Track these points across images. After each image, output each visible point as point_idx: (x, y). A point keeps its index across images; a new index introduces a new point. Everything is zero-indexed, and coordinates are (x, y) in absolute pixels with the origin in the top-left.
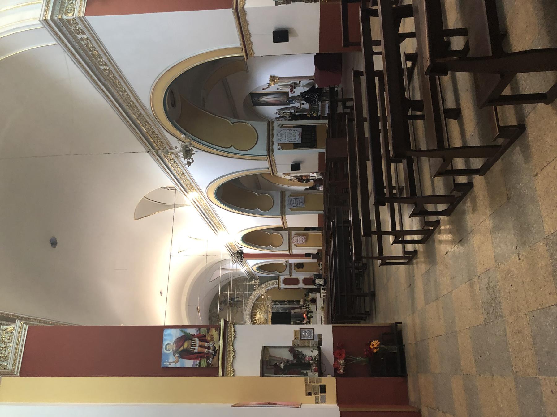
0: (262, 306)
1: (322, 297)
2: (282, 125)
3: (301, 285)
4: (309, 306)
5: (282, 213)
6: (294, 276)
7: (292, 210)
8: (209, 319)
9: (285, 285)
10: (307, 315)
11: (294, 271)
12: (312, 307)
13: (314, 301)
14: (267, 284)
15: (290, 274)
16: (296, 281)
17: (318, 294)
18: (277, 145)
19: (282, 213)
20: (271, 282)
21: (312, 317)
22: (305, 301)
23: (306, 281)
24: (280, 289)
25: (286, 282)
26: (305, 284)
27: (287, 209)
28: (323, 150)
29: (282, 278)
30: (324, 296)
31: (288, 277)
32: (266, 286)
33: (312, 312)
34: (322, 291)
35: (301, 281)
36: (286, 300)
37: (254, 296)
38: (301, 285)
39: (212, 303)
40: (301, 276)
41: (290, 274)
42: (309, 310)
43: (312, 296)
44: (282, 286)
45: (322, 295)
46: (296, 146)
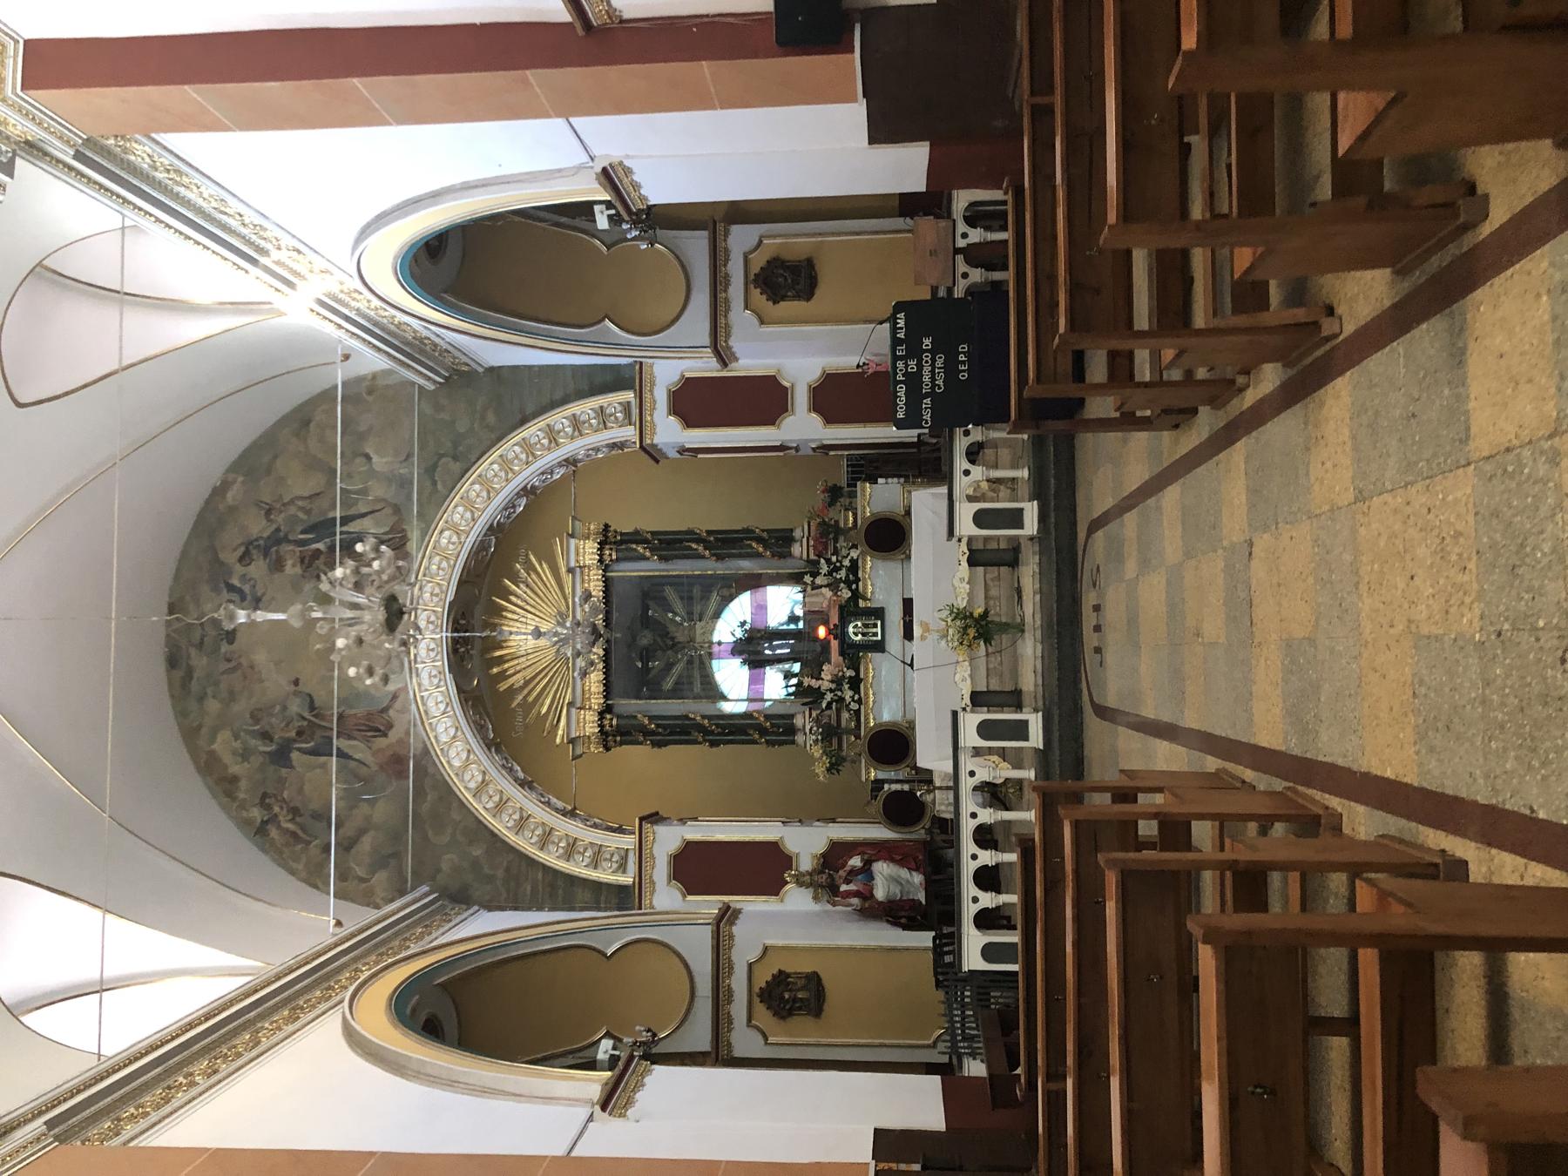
0: (544, 570)
1: (966, 526)
3: (802, 426)
4: (854, 567)
6: (750, 361)
8: (173, 662)
9: (689, 423)
10: (839, 632)
11: (740, 318)
12: (880, 581)
13: (890, 536)
14: (559, 418)
15: (723, 356)
17: (926, 504)
20: (585, 408)
21: (879, 647)
22: (828, 534)
23: (834, 396)
24: (652, 453)
25: (694, 402)
26: (830, 419)
29: (666, 373)
30: (981, 519)
31: (704, 366)
32: (552, 435)
33: (879, 613)
34: (968, 477)
35: (801, 399)
36: (702, 525)
37: (469, 504)
38: (802, 426)
39: (184, 554)
40: (795, 352)
41: (723, 356)
42: (856, 595)
43: (879, 496)
44: (669, 432)
45: (965, 513)
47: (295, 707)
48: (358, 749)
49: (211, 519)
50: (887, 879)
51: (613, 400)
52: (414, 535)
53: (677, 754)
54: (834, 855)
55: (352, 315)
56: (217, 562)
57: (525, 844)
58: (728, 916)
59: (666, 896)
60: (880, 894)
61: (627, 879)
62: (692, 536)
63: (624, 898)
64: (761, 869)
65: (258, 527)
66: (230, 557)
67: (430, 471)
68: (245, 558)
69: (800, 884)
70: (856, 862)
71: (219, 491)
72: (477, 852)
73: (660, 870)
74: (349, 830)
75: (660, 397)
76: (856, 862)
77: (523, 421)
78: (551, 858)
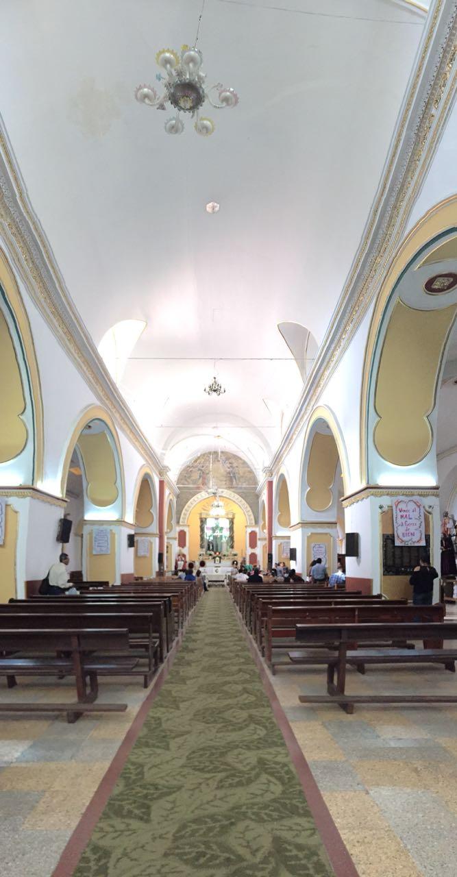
2: (430, 513)
5: (304, 524)
6: (259, 543)
7: (308, 538)
15: (259, 539)
16: (253, 544)
18: (389, 504)
19: (304, 524)
20: (252, 517)
23: (253, 556)
27: (310, 531)
28: (376, 591)
29: (257, 530)
31: (258, 537)
33: (220, 562)
35: (253, 551)
36: (235, 534)
38: (250, 551)
46: (388, 540)
47: (207, 471)
48: (201, 481)
49: (236, 458)
50: (181, 564)
51: (253, 522)
52: (233, 490)
53: (199, 529)
54: (184, 556)
55: (282, 453)
56: (230, 458)
57: (186, 507)
58: (175, 539)
59: (178, 529)
60: (179, 563)
61: (181, 523)
62: (233, 533)
63: (178, 522)
64: (182, 543)
65: (235, 465)
66: (230, 461)
67: (243, 492)
68: (230, 463)
69: (180, 550)
70: (183, 559)
71: (241, 459)
72: (185, 500)
73: (181, 528)
74: (189, 480)
75: (254, 529)
76: (183, 559)
77: (251, 507)
78: (184, 511)
